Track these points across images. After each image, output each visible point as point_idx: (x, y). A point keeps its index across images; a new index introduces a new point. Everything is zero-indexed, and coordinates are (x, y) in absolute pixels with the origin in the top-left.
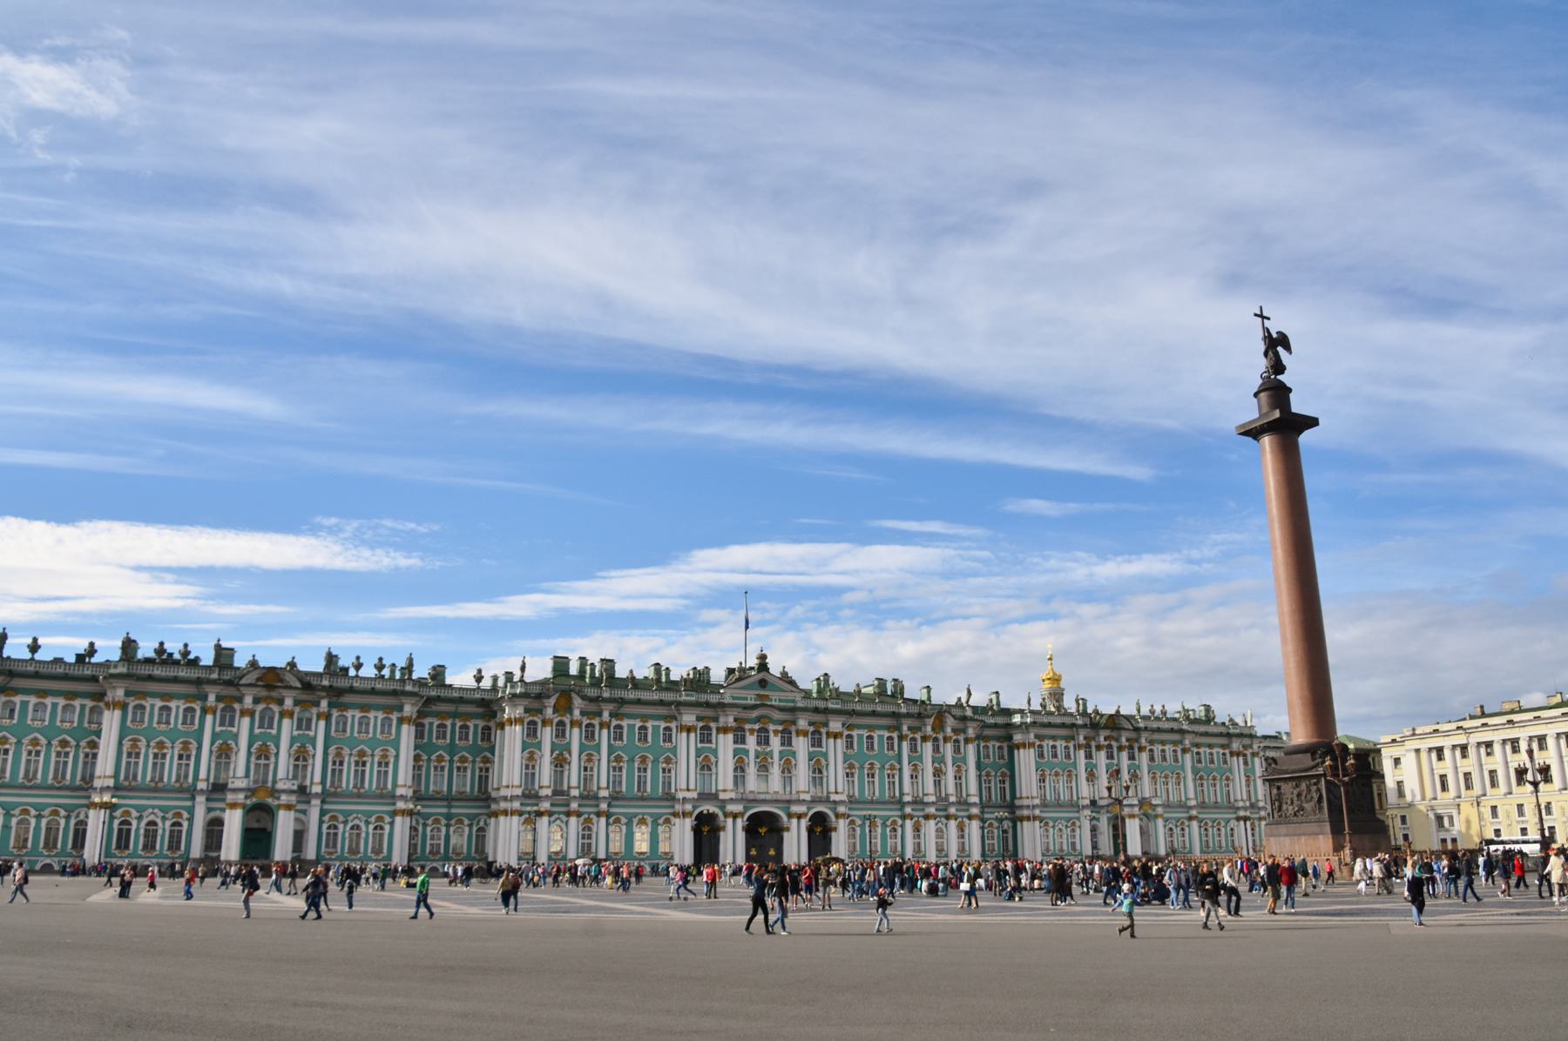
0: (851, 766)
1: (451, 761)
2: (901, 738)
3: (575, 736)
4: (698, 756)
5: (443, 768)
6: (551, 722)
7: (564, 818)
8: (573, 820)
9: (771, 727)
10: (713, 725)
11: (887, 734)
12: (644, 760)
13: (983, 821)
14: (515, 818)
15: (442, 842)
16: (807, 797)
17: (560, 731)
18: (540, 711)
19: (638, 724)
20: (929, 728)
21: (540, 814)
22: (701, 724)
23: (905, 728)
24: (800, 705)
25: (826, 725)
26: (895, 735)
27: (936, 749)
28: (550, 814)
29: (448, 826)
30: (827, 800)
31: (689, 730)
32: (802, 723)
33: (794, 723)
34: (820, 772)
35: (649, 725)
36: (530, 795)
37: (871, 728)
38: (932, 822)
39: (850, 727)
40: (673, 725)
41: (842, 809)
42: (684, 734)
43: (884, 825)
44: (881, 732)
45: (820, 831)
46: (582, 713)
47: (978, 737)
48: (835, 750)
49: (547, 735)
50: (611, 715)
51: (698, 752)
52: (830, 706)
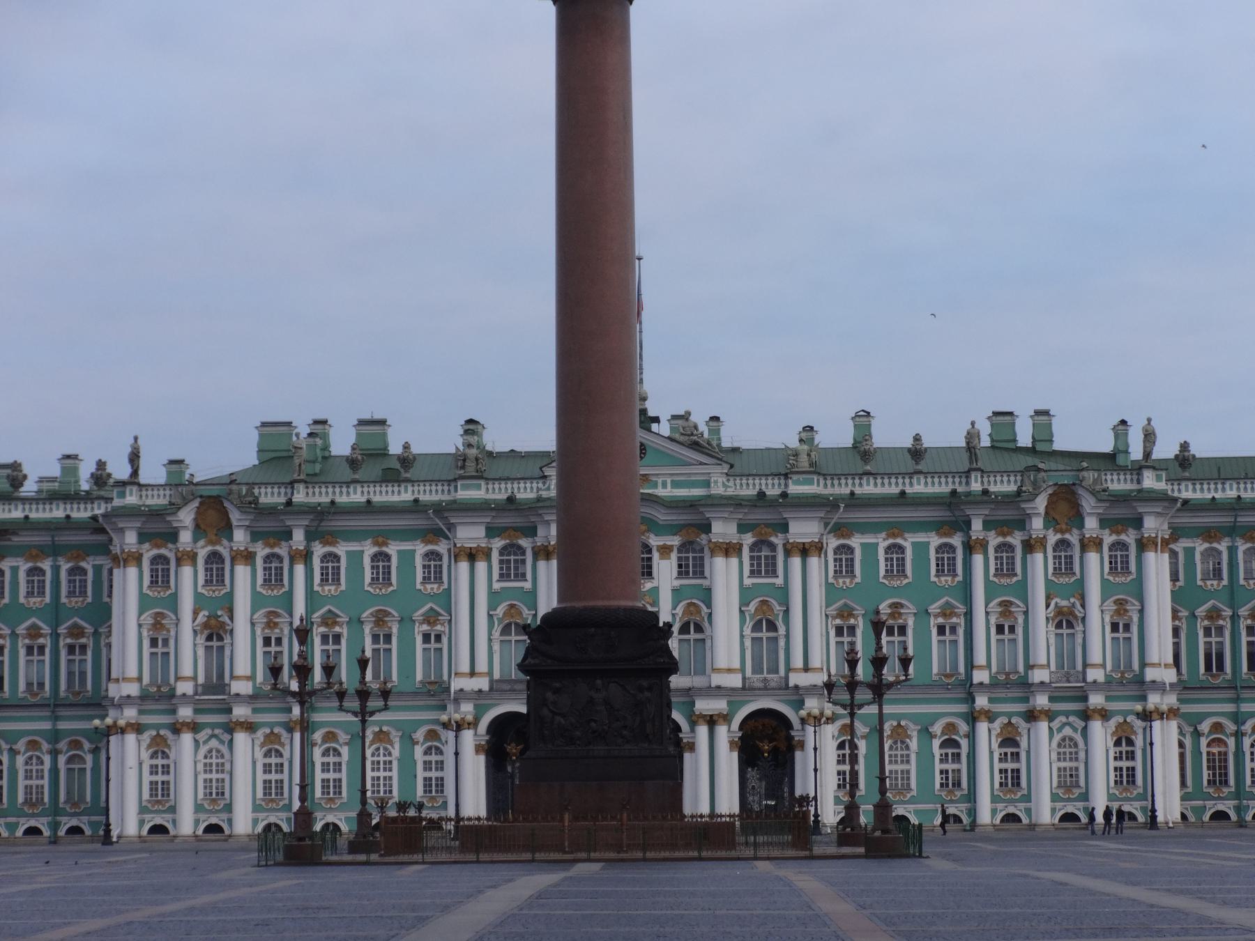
0: (846, 613)
1: (55, 636)
2: (969, 548)
3: (243, 580)
4: (492, 607)
5: (41, 649)
6: (192, 557)
7: (226, 737)
8: (241, 738)
9: (654, 541)
10: (524, 542)
11: (935, 541)
12: (380, 619)
13: (1193, 721)
14: (131, 738)
15: (46, 782)
16: (735, 681)
17: (216, 567)
18: (173, 536)
19: (369, 550)
20: (1037, 524)
21: (176, 729)
22: (497, 544)
23: (977, 525)
24: (718, 490)
25: (784, 528)
26: (956, 540)
27: (1064, 566)
28: (195, 727)
29: (55, 753)
30: (787, 687)
31: (472, 556)
32: (723, 530)
33: (707, 528)
34: (772, 626)
35: (392, 549)
36: (160, 696)
37: (896, 529)
38: (1043, 726)
39: (841, 530)
40: (442, 547)
41: (812, 705)
42: (464, 566)
43: (926, 733)
44: (921, 537)
45: (768, 746)
46: (255, 536)
47: (1177, 533)
48: (809, 583)
49: (188, 581)
50: (310, 536)
51: (494, 598)
52: (794, 489)
